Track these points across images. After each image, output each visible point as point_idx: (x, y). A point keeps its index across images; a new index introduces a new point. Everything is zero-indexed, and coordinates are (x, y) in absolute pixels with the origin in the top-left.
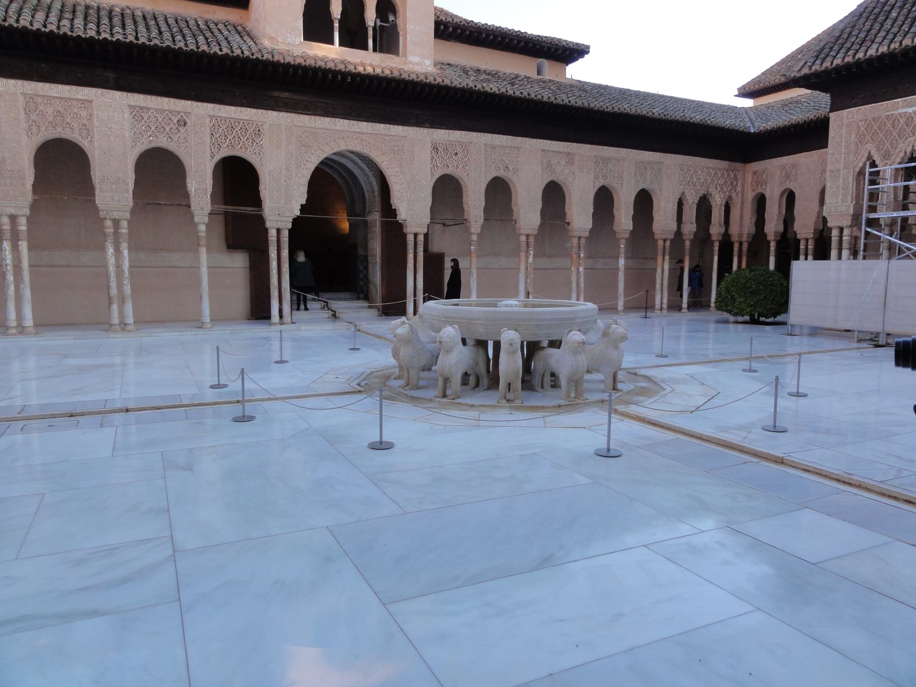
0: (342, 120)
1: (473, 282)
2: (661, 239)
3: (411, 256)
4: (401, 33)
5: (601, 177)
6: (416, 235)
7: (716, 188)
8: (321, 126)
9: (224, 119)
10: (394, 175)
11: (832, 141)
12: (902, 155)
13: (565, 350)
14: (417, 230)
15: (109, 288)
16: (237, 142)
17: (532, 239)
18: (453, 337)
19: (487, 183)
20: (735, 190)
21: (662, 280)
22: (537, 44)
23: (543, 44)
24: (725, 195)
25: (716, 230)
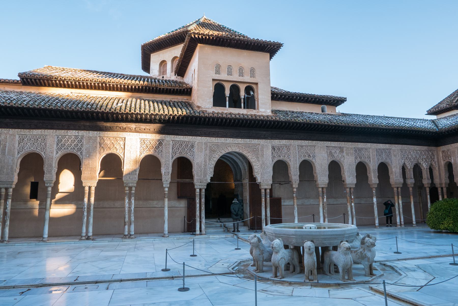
1: (296, 212)
2: (395, 187)
4: (256, 100)
5: (358, 157)
6: (265, 190)
7: (423, 160)
8: (220, 142)
9: (178, 141)
10: (254, 162)
13: (340, 252)
14: (266, 187)
15: (125, 218)
16: (183, 151)
17: (325, 190)
20: (434, 161)
22: (320, 99)
23: (323, 99)
24: (428, 164)
25: (426, 181)
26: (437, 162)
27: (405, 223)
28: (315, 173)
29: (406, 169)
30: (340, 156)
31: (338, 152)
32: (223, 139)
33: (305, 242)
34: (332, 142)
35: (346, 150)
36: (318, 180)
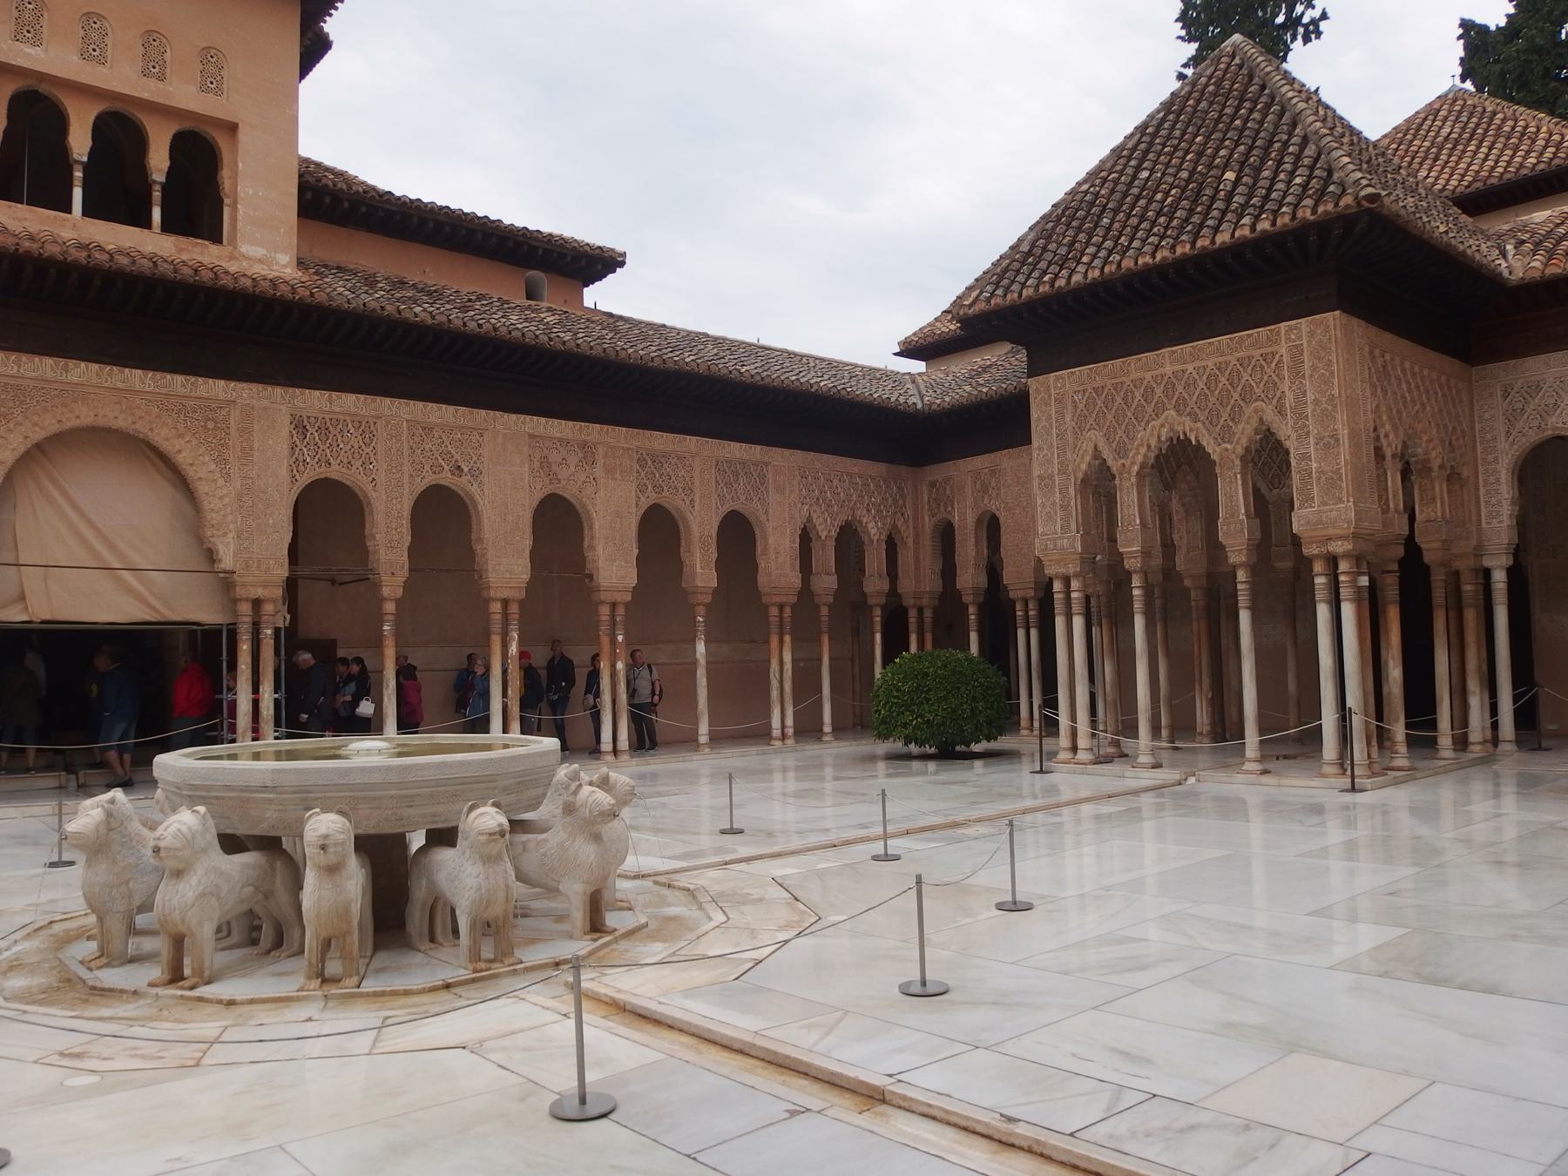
0: (83, 364)
2: (774, 605)
3: (245, 647)
4: (226, 201)
7: (868, 511)
10: (207, 480)
11: (1036, 427)
12: (1143, 450)
14: (259, 592)
17: (514, 609)
18: (189, 837)
19: (415, 495)
20: (903, 514)
21: (781, 682)
23: (535, 244)
24: (884, 524)
25: (875, 584)
26: (911, 520)
27: (796, 733)
28: (480, 540)
29: (814, 538)
30: (583, 478)
31: (573, 460)
32: (49, 361)
33: (311, 815)
34: (551, 421)
35: (606, 456)
36: (490, 569)
